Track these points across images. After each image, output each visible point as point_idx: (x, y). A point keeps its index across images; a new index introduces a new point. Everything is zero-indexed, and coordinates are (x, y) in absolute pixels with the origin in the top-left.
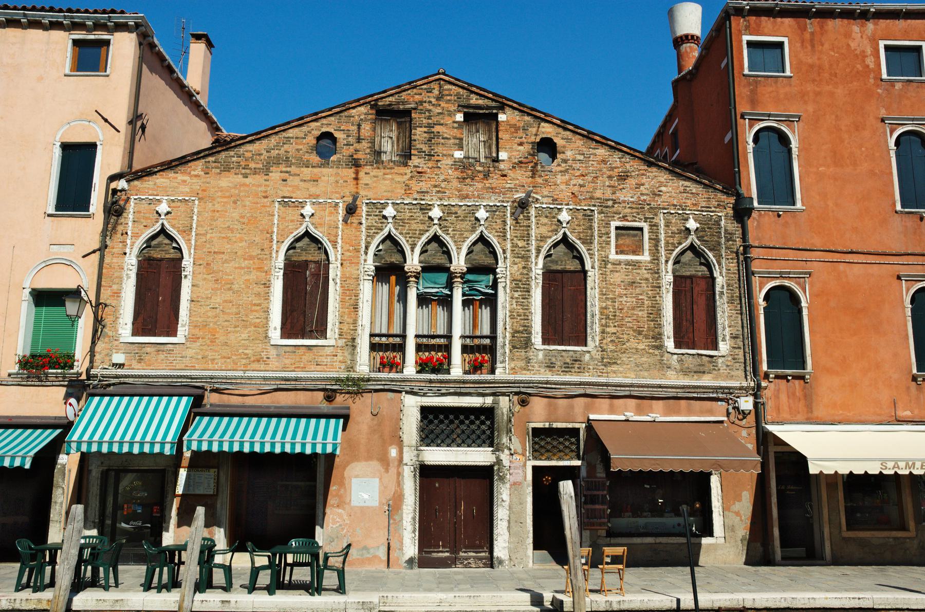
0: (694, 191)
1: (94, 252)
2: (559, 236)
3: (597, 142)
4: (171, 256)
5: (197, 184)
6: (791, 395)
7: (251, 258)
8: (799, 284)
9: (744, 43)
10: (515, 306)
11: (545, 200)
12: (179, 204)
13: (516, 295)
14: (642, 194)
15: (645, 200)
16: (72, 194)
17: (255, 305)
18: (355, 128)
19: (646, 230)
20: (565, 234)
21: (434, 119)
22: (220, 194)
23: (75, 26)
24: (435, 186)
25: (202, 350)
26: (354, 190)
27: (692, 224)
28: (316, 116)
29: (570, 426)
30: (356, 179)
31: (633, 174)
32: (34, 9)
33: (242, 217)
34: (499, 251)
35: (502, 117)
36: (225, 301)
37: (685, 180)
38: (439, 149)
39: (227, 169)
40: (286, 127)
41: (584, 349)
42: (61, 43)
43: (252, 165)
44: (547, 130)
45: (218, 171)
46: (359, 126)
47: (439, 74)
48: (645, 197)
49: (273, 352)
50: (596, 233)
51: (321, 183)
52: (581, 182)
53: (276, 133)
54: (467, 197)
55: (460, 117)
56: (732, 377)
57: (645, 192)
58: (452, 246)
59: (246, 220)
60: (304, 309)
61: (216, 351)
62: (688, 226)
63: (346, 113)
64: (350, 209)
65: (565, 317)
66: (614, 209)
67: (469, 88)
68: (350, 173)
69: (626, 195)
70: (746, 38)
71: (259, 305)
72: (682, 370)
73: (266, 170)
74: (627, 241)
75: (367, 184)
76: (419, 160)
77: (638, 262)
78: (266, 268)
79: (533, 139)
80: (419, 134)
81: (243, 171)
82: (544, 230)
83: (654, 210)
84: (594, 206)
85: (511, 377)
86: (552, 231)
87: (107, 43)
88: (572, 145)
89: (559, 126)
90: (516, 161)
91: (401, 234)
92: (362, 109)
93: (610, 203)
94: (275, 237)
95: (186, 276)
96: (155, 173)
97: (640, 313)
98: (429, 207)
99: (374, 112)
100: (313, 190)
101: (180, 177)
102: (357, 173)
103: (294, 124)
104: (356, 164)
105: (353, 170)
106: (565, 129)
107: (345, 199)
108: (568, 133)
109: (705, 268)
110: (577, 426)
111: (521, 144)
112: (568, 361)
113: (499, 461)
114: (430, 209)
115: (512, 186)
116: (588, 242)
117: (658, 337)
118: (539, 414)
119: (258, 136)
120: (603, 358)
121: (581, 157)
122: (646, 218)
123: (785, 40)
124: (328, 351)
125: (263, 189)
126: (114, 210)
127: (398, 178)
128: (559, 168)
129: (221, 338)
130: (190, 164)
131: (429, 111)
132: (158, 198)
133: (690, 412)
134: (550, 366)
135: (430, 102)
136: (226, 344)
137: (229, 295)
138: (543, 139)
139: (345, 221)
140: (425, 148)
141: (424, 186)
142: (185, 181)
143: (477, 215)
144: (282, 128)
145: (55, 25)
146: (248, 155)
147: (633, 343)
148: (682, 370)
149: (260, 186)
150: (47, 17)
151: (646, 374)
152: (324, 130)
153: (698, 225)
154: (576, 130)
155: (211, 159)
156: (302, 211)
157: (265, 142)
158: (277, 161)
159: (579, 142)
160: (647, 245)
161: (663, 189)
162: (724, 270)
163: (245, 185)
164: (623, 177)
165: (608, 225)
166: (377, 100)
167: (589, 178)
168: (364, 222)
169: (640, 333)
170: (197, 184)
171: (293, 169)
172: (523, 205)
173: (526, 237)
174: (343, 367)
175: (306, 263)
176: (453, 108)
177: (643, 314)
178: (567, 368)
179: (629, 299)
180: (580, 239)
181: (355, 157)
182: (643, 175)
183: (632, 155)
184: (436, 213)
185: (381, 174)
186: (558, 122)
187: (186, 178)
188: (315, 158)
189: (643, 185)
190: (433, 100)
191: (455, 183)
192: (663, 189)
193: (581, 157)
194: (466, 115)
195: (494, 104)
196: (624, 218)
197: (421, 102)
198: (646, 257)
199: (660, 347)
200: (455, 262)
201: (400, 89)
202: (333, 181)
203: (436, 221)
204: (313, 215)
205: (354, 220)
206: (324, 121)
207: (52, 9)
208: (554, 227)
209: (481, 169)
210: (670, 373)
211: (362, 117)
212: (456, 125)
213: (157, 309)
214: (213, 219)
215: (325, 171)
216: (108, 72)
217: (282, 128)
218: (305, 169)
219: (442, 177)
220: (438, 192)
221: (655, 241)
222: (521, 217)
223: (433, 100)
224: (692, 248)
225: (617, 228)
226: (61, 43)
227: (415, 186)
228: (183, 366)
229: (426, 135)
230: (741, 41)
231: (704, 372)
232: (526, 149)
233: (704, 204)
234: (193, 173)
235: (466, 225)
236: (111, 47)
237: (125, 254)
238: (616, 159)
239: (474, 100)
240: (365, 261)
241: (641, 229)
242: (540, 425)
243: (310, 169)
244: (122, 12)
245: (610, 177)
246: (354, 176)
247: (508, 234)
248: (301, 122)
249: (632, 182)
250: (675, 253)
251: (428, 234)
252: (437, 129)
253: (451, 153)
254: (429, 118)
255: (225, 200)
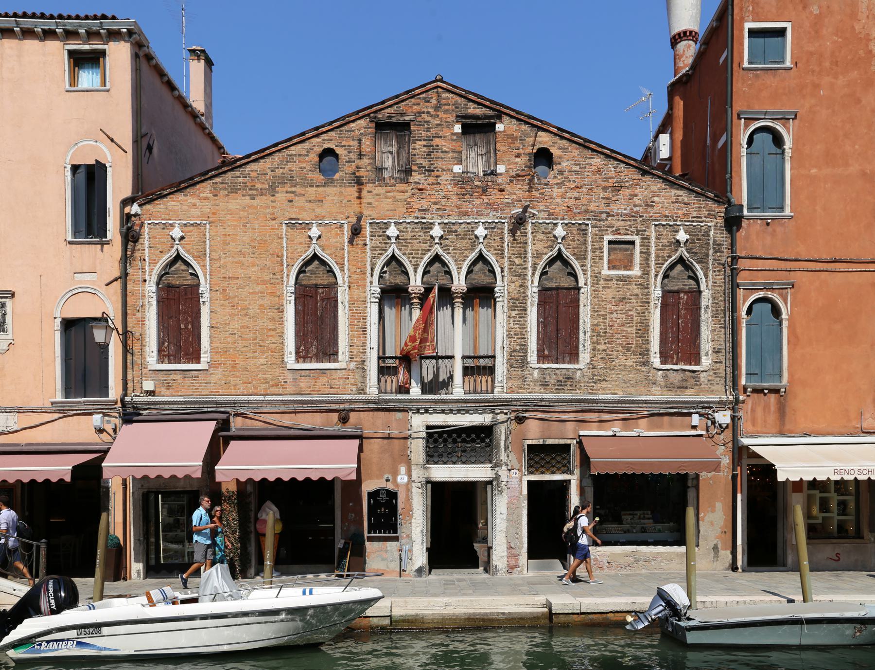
0: (686, 200)
1: (116, 280)
2: (555, 252)
3: (593, 150)
4: (189, 282)
5: (207, 207)
6: (766, 407)
7: (264, 283)
8: (781, 295)
9: (746, 31)
10: (512, 325)
11: (541, 215)
12: (191, 228)
13: (513, 314)
14: (635, 206)
15: (637, 212)
16: (89, 220)
17: (271, 330)
18: (356, 143)
19: (638, 243)
20: (560, 249)
21: (433, 132)
22: (229, 217)
23: (70, 34)
24: (436, 204)
25: (224, 376)
26: (359, 210)
27: (682, 236)
28: (318, 132)
29: (562, 442)
30: (359, 198)
31: (627, 184)
32: (25, 15)
33: (253, 240)
34: (497, 270)
35: (499, 127)
36: (243, 327)
37: (677, 189)
38: (439, 164)
39: (234, 191)
40: (288, 144)
41: (576, 366)
42: (56, 52)
43: (259, 186)
44: (544, 140)
45: (226, 192)
46: (360, 140)
47: (436, 81)
48: (638, 209)
49: (290, 376)
50: (590, 248)
51: (326, 204)
52: (576, 194)
53: (279, 151)
54: (466, 214)
55: (458, 128)
56: (712, 392)
57: (638, 202)
58: (453, 267)
59: (256, 244)
60: (317, 331)
61: (236, 377)
62: (678, 238)
63: (346, 127)
64: (356, 230)
65: (559, 332)
66: (608, 223)
67: (466, 95)
68: (353, 191)
69: (620, 207)
70: (748, 25)
71: (274, 330)
72: (666, 386)
73: (272, 190)
74: (619, 255)
75: (370, 204)
76: (419, 177)
77: (629, 277)
78: (278, 293)
79: (529, 150)
80: (419, 147)
81: (250, 192)
82: (540, 247)
83: (647, 221)
84: (589, 219)
85: (508, 396)
86: (547, 247)
87: (103, 53)
88: (569, 155)
89: (556, 134)
90: (514, 174)
91: (404, 254)
92: (362, 122)
93: (604, 216)
94: (285, 261)
95: (204, 302)
96: (165, 196)
97: (629, 330)
98: (430, 226)
99: (373, 125)
100: (319, 211)
101: (191, 200)
102: (360, 191)
103: (295, 141)
104: (359, 182)
105: (355, 189)
106: (562, 138)
107: (350, 220)
108: (565, 142)
109: (692, 282)
110: (568, 442)
111: (518, 156)
112: (561, 378)
113: (497, 477)
114: (431, 228)
115: (509, 201)
116: (581, 258)
117: (646, 353)
118: (534, 432)
119: (262, 154)
120: (594, 375)
121: (577, 168)
122: (638, 231)
123: (788, 25)
124: (340, 374)
125: (270, 210)
126: (130, 237)
127: (400, 196)
128: (556, 181)
129: (241, 364)
130: (198, 186)
131: (428, 122)
132: (171, 222)
133: (672, 427)
134: (544, 384)
135: (428, 113)
136: (246, 369)
137: (246, 321)
138: (539, 150)
139: (351, 242)
140: (425, 163)
141: (425, 204)
142: (194, 204)
143: (476, 233)
144: (285, 145)
145: (49, 34)
146: (254, 174)
147: (621, 361)
148: (666, 386)
149: (267, 207)
150: (40, 25)
151: (632, 390)
152: (326, 146)
153: (688, 237)
154: (572, 138)
155: (218, 180)
156: (309, 233)
157: (269, 160)
158: (282, 181)
159: (575, 151)
160: (637, 258)
161: (656, 199)
162: (710, 283)
163: (252, 207)
164: (617, 189)
165: (601, 239)
166: (376, 112)
167: (584, 190)
168: (368, 243)
169: (628, 350)
170: (207, 207)
171: (298, 189)
172: (519, 222)
173: (523, 255)
174: (354, 389)
175: (316, 286)
176: (451, 118)
177: (633, 330)
178: (560, 385)
179: (619, 316)
180: (574, 255)
181: (357, 174)
182: (637, 184)
183: (627, 164)
184: (437, 231)
185: (383, 192)
186: (555, 130)
187: (196, 201)
188: (318, 177)
189: (636, 196)
190: (431, 110)
191: (455, 200)
192: (656, 199)
193: (577, 168)
194: (464, 126)
195: (491, 113)
196: (617, 232)
197: (420, 113)
198: (636, 271)
199: (646, 363)
200: (456, 282)
201: (398, 99)
202: (336, 201)
203: (437, 241)
204: (320, 237)
205: (358, 241)
206: (325, 137)
207: (43, 16)
208: (550, 243)
209: (479, 183)
210: (655, 389)
211: (362, 131)
212: (454, 137)
213: (180, 334)
214: (225, 243)
215: (329, 190)
216: (108, 87)
217: (285, 145)
218: (309, 189)
219: (442, 194)
220: (438, 209)
221: (646, 254)
222: (518, 233)
223: (431, 110)
224: (681, 260)
225: (610, 242)
226: (56, 52)
227: (417, 204)
228: (207, 392)
229: (425, 149)
230: (742, 29)
231: (686, 388)
232: (522, 161)
233: (695, 214)
234: (202, 195)
235: (466, 243)
236: (107, 58)
237: (145, 281)
238: (610, 169)
239: (472, 109)
240: (371, 283)
241: (632, 243)
242: (535, 442)
243: (315, 188)
244: (114, 18)
245: (605, 189)
246: (357, 195)
247: (506, 251)
248: (302, 138)
249: (625, 193)
250: (664, 266)
251: (429, 254)
252: (437, 141)
253: (450, 167)
254: (428, 130)
255: (235, 223)
